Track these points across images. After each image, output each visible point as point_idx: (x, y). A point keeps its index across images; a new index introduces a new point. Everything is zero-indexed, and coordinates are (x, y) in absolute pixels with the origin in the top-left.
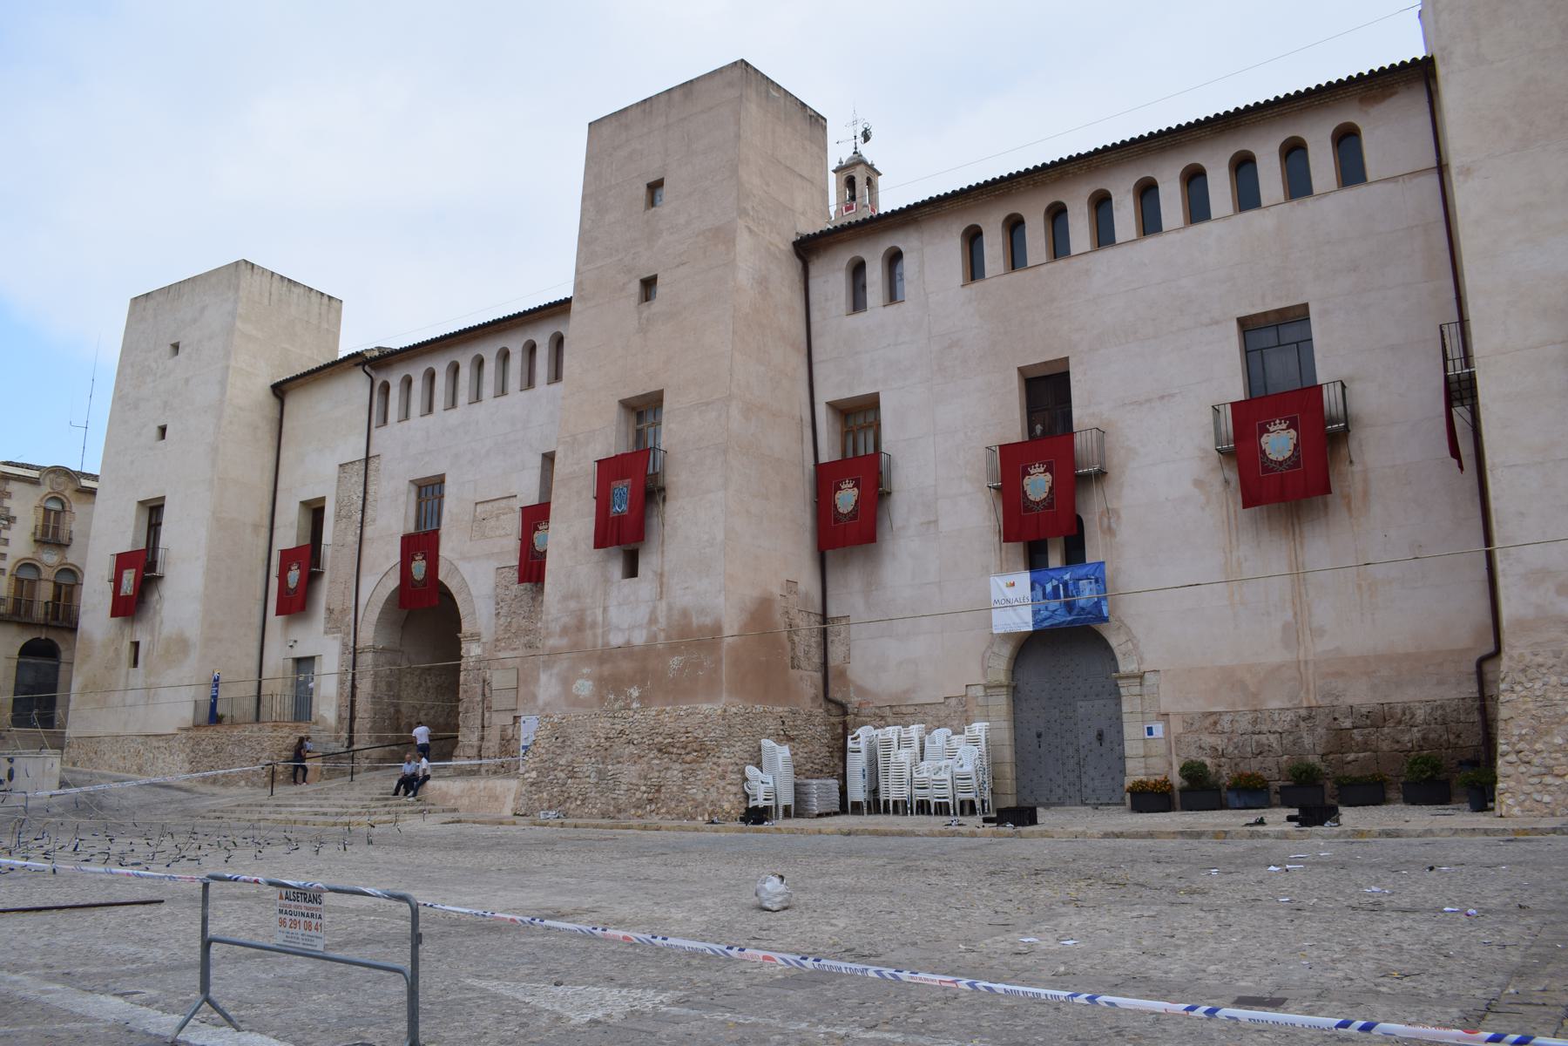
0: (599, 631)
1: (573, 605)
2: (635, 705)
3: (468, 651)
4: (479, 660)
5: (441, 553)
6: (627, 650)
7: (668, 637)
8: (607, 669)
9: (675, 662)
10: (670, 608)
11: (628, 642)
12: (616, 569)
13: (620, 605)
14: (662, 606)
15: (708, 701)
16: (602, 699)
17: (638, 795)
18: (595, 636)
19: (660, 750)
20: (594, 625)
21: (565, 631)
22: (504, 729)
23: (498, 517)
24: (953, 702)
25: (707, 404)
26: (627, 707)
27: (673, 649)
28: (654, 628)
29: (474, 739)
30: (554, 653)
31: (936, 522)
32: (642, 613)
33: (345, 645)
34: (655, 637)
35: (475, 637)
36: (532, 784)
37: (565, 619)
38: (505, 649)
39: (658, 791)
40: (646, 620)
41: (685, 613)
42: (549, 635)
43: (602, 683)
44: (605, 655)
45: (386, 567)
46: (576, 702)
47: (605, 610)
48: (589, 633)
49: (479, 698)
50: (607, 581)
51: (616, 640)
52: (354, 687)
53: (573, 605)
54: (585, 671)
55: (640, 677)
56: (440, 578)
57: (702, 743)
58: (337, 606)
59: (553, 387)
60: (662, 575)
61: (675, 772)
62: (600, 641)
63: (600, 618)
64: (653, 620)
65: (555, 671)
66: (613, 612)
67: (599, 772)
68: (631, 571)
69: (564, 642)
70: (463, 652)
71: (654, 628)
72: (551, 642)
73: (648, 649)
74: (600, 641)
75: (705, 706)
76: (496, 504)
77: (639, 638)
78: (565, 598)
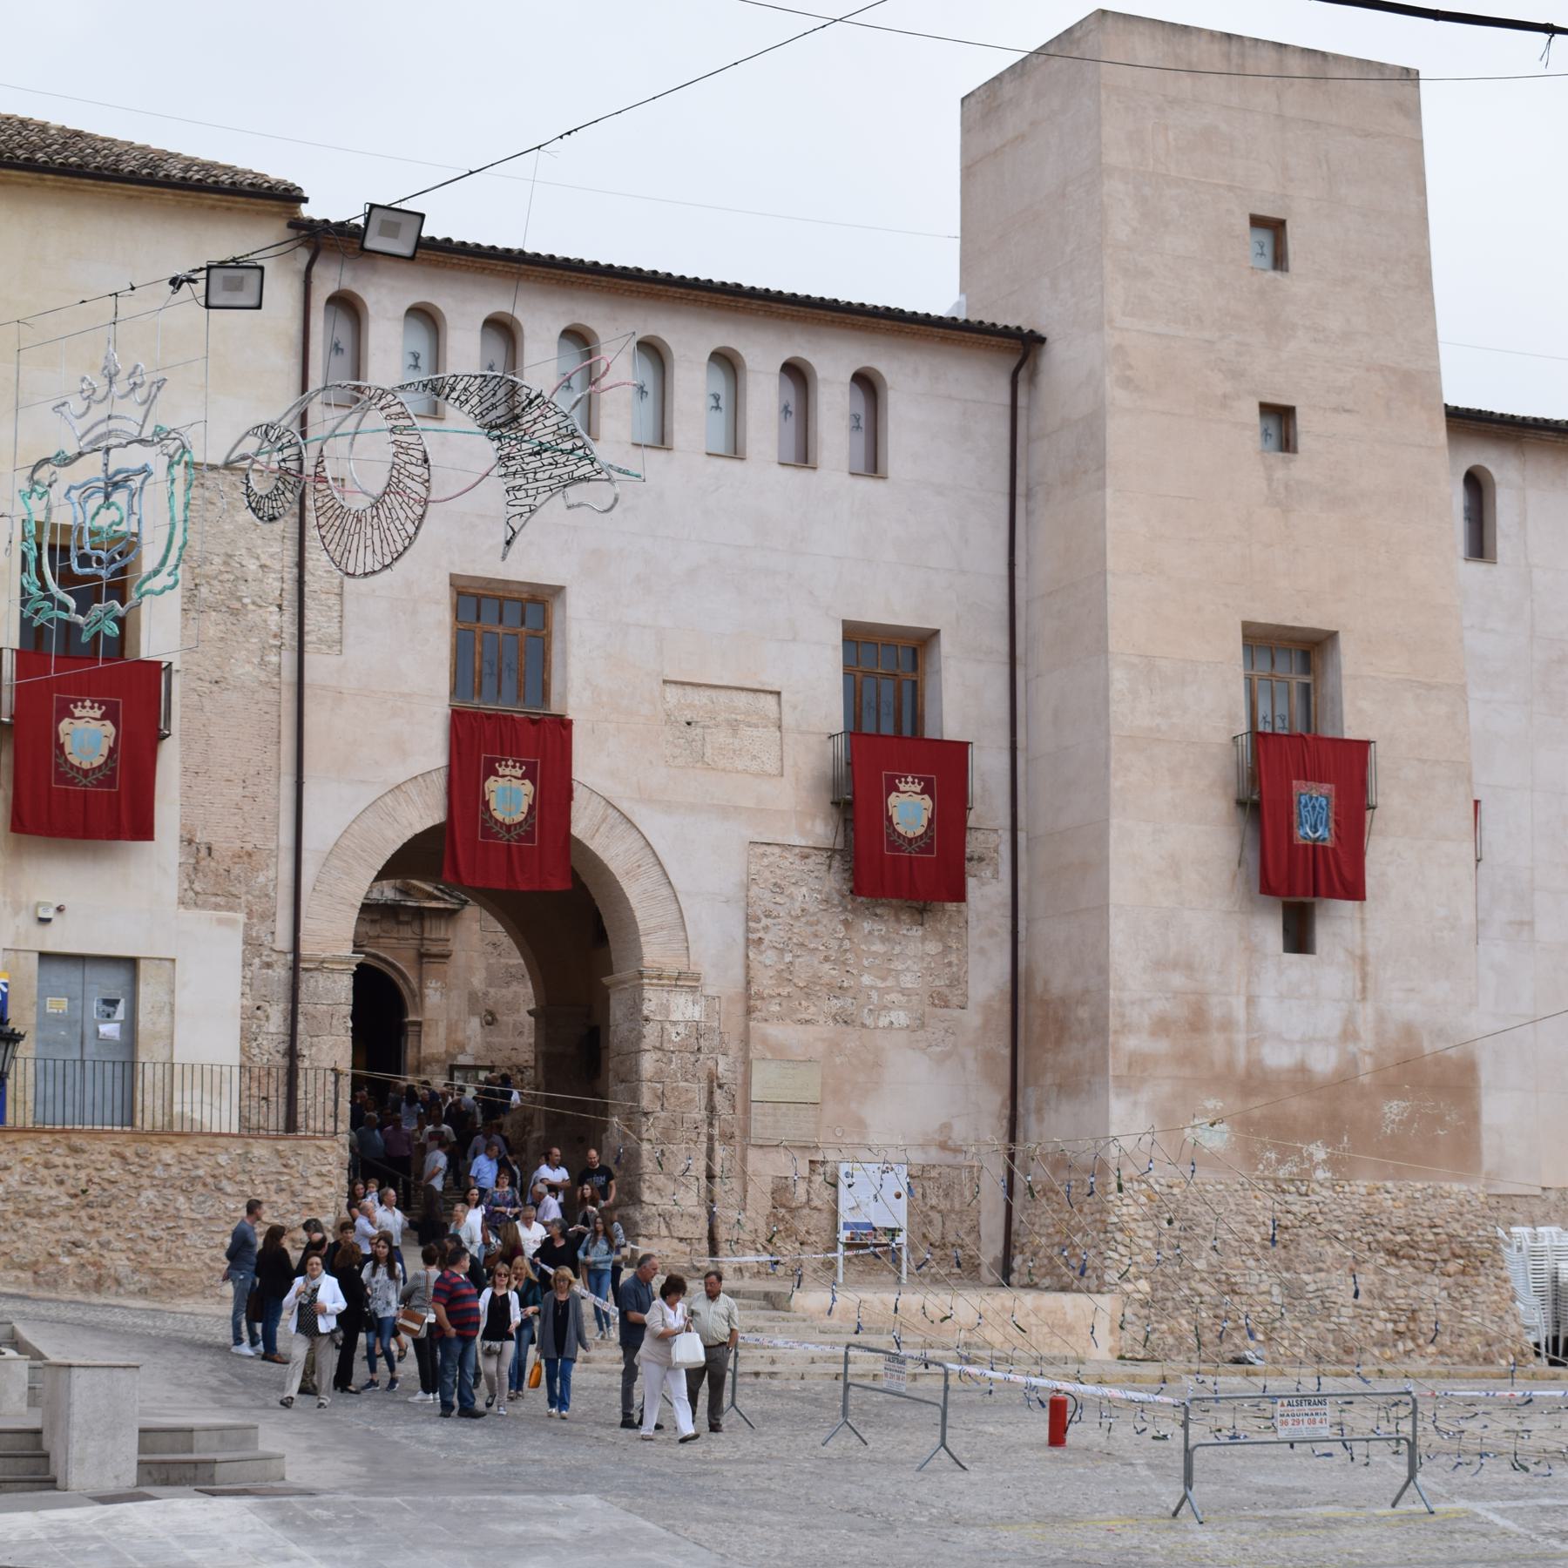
0: (1240, 1038)
1: (1177, 980)
2: (1320, 1174)
3: (666, 1008)
4: (698, 1031)
5: (578, 774)
6: (1301, 1079)
7: (1379, 1069)
8: (1257, 1106)
9: (1394, 1109)
10: (1381, 1018)
11: (1302, 1069)
12: (1271, 931)
13: (1281, 997)
14: (1366, 1015)
15: (1460, 1179)
16: (1251, 1159)
17: (1378, 1325)
18: (1230, 1044)
19: (1393, 1253)
20: (1227, 1025)
21: (1162, 1026)
22: (780, 1191)
23: (734, 726)
24: (1553, 1196)
25: (1430, 687)
26: (1305, 1177)
27: (1391, 1089)
28: (1351, 1047)
29: (690, 1200)
30: (1140, 1064)
31: (1531, 924)
32: (1329, 1018)
33: (252, 944)
34: (1354, 1062)
35: (686, 981)
36: (1145, 1304)
37: (1160, 1006)
38: (780, 1018)
39: (1413, 1319)
40: (1336, 1030)
41: (1408, 1031)
42: (1126, 1028)
43: (1246, 1126)
44: (1253, 1082)
45: (400, 774)
46: (1194, 1160)
47: (1251, 1001)
48: (1217, 1041)
49: (700, 1114)
50: (1252, 950)
51: (1278, 1058)
52: (292, 1054)
53: (1177, 980)
54: (1212, 1104)
55: (1331, 1127)
56: (579, 829)
57: (1466, 1246)
58: (223, 835)
59: (788, 473)
60: (1363, 960)
61: (1433, 1289)
62: (1241, 1058)
63: (1240, 1014)
64: (1349, 1034)
65: (1145, 1096)
66: (1269, 1009)
67: (1286, 1286)
68: (1299, 939)
69: (1162, 1046)
70: (648, 1008)
71: (1351, 1047)
72: (1131, 1043)
73: (1343, 1081)
74: (1241, 1058)
75: (1456, 1187)
76: (723, 696)
77: (1324, 1062)
78: (1160, 965)
